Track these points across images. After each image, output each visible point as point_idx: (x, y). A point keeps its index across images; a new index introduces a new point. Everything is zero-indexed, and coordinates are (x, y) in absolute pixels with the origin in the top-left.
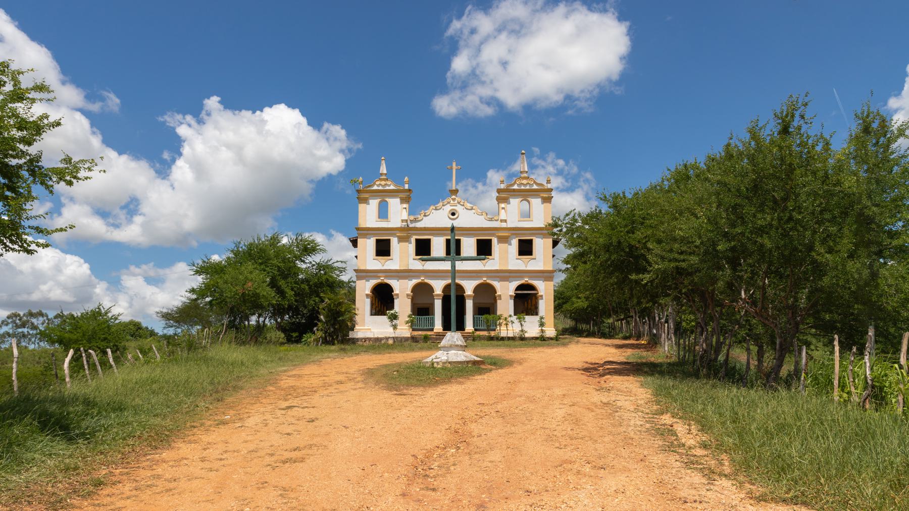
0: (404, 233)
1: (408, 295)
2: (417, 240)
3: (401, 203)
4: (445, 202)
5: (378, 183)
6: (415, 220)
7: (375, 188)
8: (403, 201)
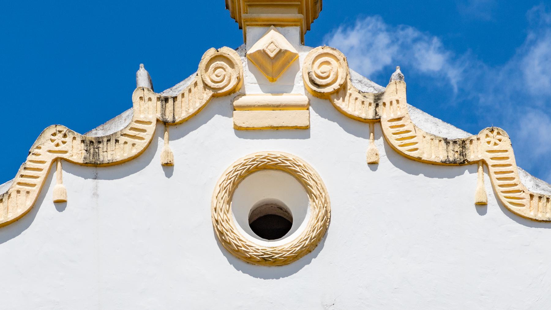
4: (190, 95)
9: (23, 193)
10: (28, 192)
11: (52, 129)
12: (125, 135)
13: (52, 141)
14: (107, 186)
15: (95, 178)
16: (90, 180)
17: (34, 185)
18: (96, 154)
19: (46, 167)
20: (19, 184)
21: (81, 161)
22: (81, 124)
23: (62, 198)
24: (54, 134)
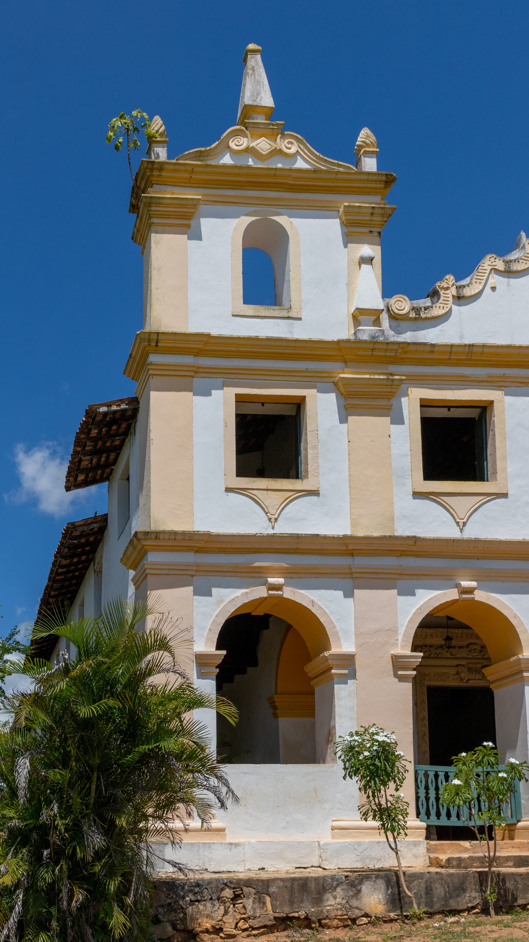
0: (369, 372)
1: (398, 663)
2: (425, 404)
3: (349, 238)
5: (240, 143)
6: (418, 320)
7: (227, 160)
8: (354, 229)
9: (478, 283)
10: (480, 283)
11: (490, 256)
12: (522, 259)
13: (490, 261)
14: (514, 281)
15: (508, 278)
16: (506, 279)
17: (483, 280)
18: (509, 267)
19: (488, 271)
20: (476, 279)
21: (503, 270)
22: (501, 253)
23: (495, 286)
24: (490, 258)
